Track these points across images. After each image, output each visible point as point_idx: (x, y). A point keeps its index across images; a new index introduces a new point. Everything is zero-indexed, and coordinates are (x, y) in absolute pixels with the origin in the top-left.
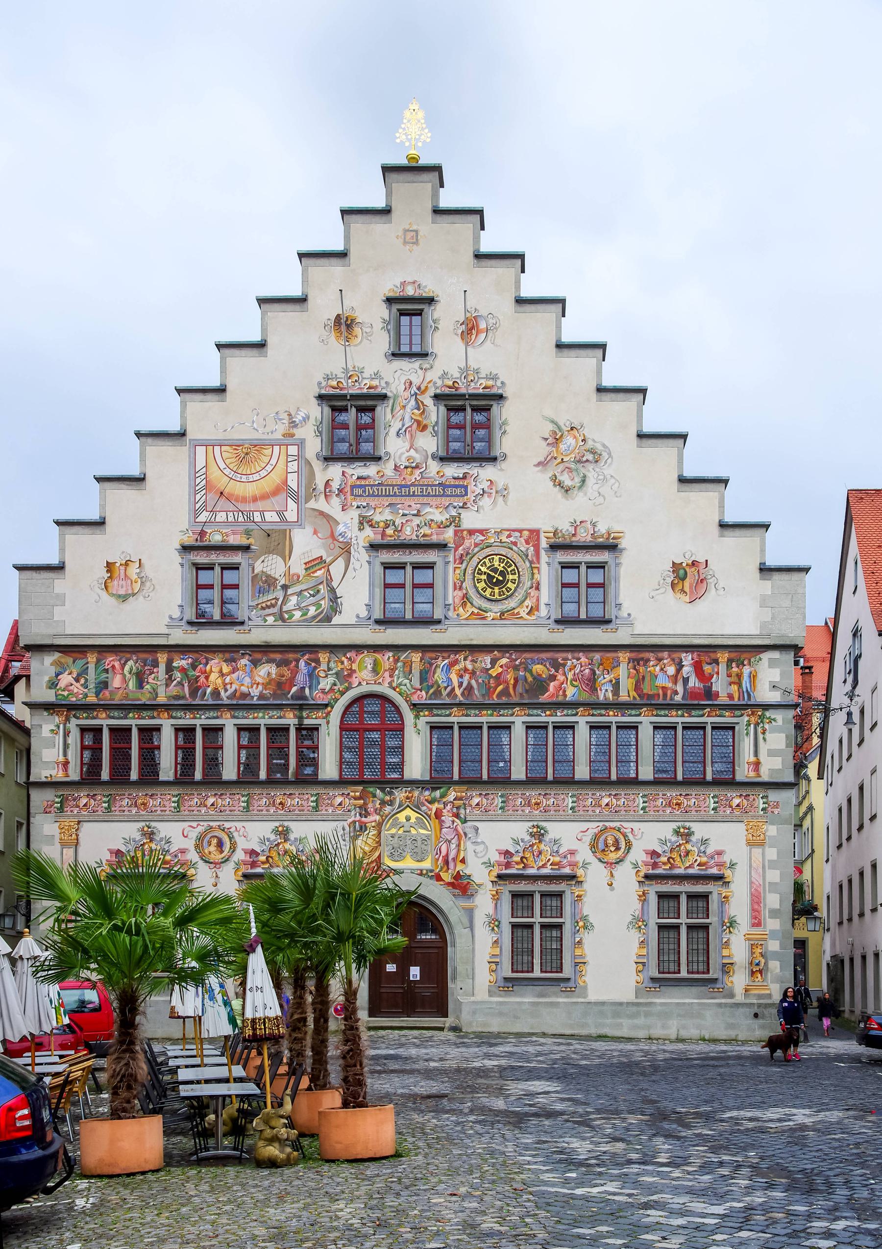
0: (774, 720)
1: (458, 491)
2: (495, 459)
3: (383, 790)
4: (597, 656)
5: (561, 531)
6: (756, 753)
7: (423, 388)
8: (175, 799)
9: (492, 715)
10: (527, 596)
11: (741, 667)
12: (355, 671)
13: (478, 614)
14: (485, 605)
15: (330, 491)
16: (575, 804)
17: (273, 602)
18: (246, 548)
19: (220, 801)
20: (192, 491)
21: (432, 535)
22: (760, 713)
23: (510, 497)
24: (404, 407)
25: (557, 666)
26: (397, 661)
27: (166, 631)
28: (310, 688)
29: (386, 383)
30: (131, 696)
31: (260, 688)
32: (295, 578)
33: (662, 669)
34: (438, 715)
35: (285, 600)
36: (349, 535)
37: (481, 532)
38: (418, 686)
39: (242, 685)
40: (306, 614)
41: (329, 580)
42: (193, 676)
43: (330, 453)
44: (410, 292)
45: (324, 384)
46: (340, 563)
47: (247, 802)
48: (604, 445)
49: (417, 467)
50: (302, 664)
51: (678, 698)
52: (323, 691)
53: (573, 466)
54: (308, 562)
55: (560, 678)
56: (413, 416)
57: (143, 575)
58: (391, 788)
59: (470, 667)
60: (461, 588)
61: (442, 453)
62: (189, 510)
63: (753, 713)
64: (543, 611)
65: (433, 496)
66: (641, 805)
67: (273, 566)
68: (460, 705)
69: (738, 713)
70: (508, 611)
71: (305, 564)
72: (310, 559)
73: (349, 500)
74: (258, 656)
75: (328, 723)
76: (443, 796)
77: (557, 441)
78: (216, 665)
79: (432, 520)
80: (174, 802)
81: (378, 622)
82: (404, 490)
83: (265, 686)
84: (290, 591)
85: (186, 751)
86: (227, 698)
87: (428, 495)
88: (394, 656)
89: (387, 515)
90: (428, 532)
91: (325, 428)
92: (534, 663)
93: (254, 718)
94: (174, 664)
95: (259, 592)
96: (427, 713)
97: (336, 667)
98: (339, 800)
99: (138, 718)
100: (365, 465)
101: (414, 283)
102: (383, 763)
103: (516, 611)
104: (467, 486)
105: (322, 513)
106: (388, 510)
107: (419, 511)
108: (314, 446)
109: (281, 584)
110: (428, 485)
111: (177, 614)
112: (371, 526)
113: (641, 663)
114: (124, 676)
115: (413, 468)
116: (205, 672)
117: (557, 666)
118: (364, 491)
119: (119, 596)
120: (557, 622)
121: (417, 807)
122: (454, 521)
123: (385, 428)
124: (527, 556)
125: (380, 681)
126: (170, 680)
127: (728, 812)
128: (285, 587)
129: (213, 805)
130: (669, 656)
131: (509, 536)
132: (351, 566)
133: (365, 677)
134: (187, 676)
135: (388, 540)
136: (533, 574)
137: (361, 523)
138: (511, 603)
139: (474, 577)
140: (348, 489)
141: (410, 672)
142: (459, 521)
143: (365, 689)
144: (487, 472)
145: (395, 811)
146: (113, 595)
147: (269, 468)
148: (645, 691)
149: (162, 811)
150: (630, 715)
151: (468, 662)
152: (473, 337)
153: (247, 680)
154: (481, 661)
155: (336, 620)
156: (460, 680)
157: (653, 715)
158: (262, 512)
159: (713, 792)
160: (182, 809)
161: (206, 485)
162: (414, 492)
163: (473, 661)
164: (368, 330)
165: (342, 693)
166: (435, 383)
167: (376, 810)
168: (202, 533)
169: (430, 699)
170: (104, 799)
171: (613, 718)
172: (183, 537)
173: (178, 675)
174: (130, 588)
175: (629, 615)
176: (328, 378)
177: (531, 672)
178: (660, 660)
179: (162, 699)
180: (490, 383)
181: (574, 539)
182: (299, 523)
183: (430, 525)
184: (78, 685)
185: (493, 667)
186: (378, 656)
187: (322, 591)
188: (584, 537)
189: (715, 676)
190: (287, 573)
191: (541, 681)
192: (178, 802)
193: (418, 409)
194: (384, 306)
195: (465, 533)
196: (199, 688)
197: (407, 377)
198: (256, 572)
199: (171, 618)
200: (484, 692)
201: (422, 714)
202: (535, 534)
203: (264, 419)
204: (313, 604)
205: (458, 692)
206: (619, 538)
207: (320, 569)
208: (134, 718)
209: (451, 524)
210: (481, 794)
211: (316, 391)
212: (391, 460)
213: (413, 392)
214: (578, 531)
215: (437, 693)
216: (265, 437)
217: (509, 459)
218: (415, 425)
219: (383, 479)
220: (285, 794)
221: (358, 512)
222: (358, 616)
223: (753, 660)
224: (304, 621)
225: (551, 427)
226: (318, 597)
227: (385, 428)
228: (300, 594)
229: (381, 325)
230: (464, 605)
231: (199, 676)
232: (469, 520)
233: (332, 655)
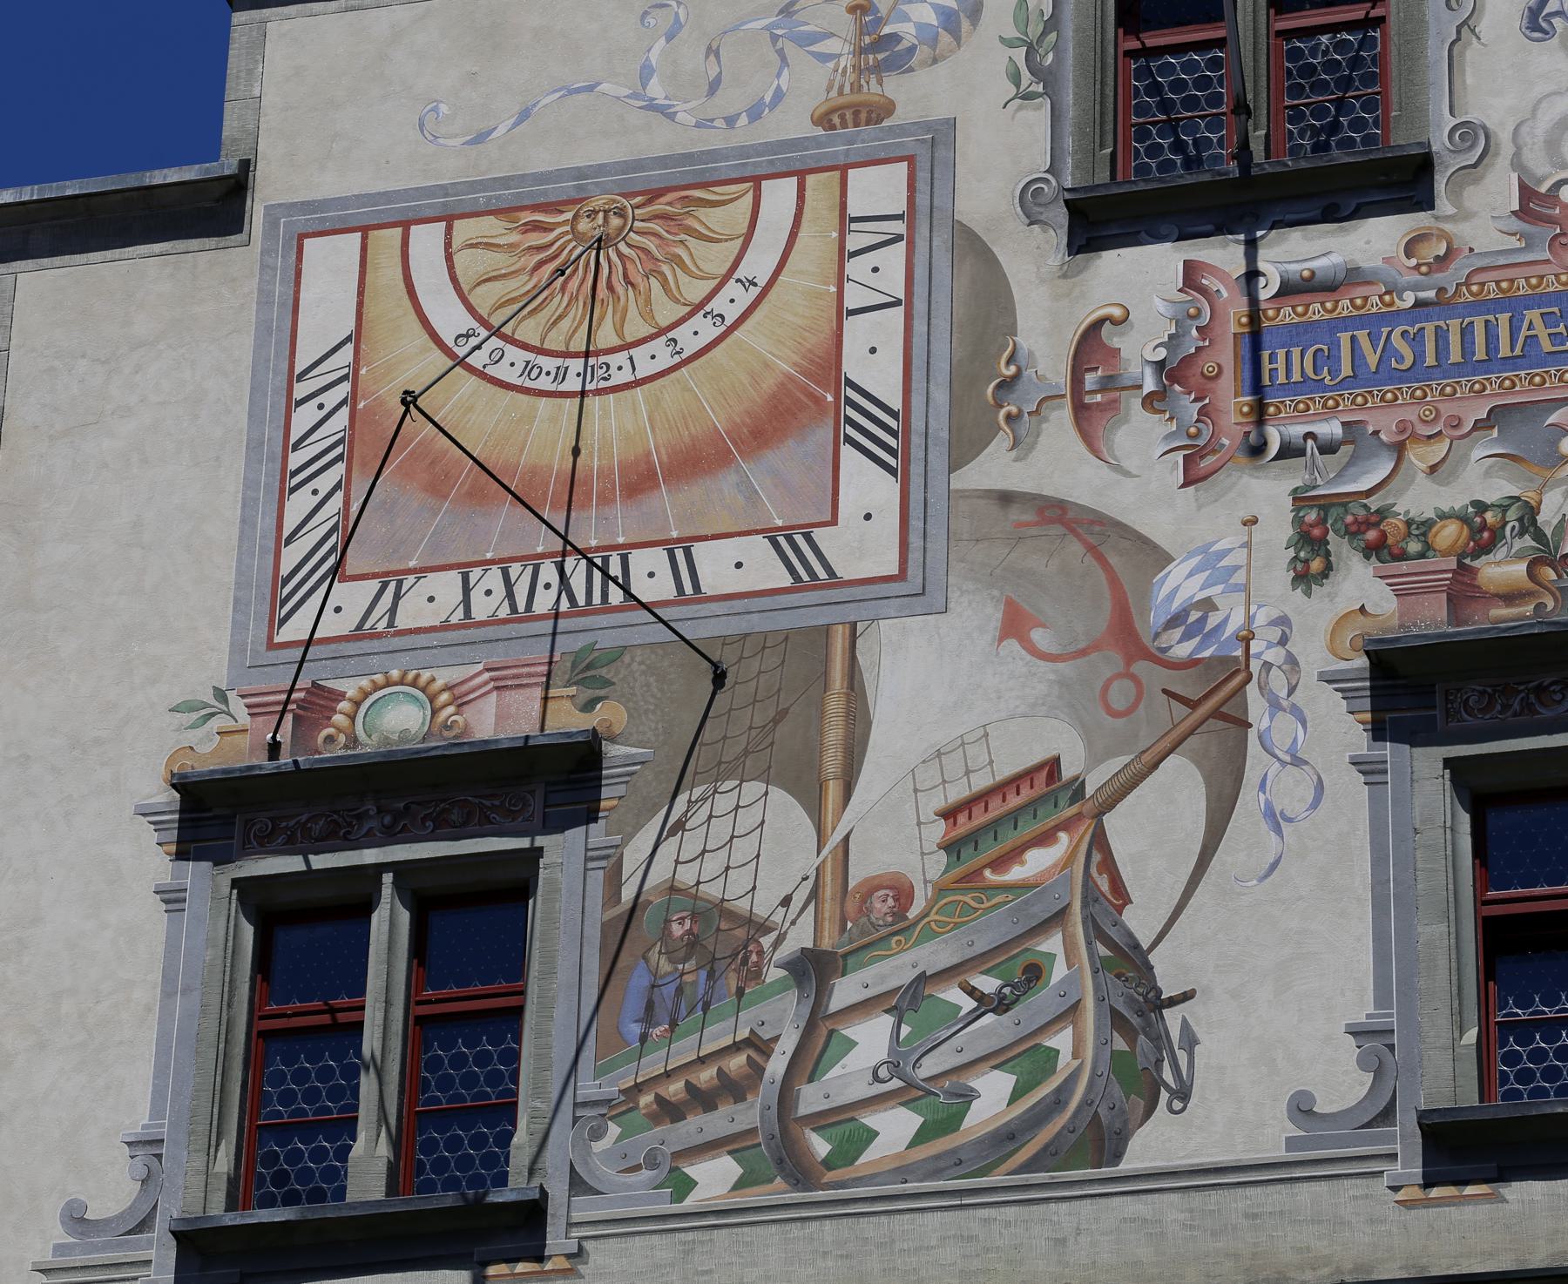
15: (1107, 384)
17: (737, 1063)
20: (267, 474)
32: (881, 906)
43: (1103, 176)
54: (967, 805)
62: (241, 584)
67: (743, 850)
71: (949, 814)
72: (981, 782)
84: (845, 992)
95: (649, 1015)
112: (1377, 550)
132: (1249, 801)
158: (680, 549)
161: (349, 439)
172: (192, 737)
187: (1059, 971)
199: (76, 1219)
203: (713, 52)
204: (996, 1059)
212: (1503, 161)
216: (715, 140)
219: (1450, 277)
221: (1292, 477)
222: (1302, 1109)
224: (935, 1168)
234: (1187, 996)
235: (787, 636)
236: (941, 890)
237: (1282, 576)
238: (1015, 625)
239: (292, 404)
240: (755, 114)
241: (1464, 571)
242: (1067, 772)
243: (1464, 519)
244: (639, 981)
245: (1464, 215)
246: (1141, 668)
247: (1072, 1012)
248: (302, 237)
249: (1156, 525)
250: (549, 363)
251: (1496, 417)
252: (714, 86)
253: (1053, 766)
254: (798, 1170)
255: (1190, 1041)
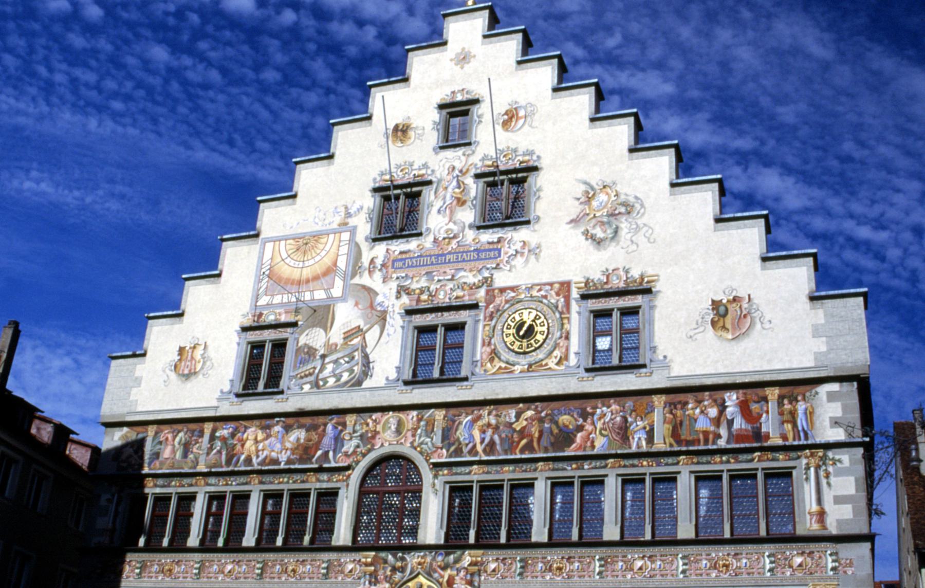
0: (840, 461)
1: (492, 254)
2: (528, 222)
3: (395, 556)
4: (629, 403)
5: (593, 281)
6: (819, 501)
7: (464, 170)
8: (197, 566)
9: (514, 471)
10: (556, 346)
11: (794, 403)
12: (378, 433)
13: (506, 368)
14: (512, 358)
16: (603, 569)
17: (311, 371)
18: (294, 325)
19: (236, 567)
20: (257, 280)
21: (464, 296)
22: (821, 454)
23: (542, 254)
24: (446, 188)
25: (585, 415)
26: (420, 420)
27: (215, 404)
28: (334, 451)
29: (433, 171)
30: (176, 466)
31: (289, 452)
32: (333, 347)
33: (702, 412)
34: (457, 474)
35: (323, 368)
36: (386, 304)
37: (512, 289)
38: (440, 445)
39: (273, 451)
40: (338, 380)
41: (364, 347)
42: (231, 444)
44: (459, 98)
45: (378, 179)
46: (376, 329)
47: (262, 569)
48: (636, 198)
49: (455, 237)
50: (329, 427)
51: (722, 443)
52: (346, 455)
53: (605, 219)
55: (589, 427)
56: (454, 195)
57: (206, 355)
58: (403, 554)
59: (493, 422)
60: (489, 344)
61: (478, 224)
63: (812, 455)
64: (573, 361)
65: (468, 261)
66: (681, 569)
67: (316, 338)
68: (480, 463)
69: (793, 454)
70: (536, 363)
71: (344, 333)
72: (349, 329)
73: (390, 273)
74: (291, 421)
75: (348, 485)
76: (457, 561)
77: (589, 200)
78: (252, 432)
79: (465, 283)
80: (196, 569)
81: (406, 383)
82: (440, 258)
83: (293, 451)
84: (327, 360)
85: (214, 517)
86: (259, 464)
87: (464, 261)
88: (417, 416)
89: (423, 283)
90: (460, 293)
91: (375, 216)
92: (561, 414)
93: (280, 483)
94: (218, 434)
95: (300, 364)
96: (446, 472)
97: (361, 429)
98: (350, 566)
99: (179, 486)
100: (407, 241)
101: (463, 90)
102: (400, 527)
103: (544, 363)
104: (499, 250)
105: (364, 287)
106: (424, 279)
107: (453, 276)
108: (364, 228)
109: (320, 354)
110: (463, 252)
111: (227, 388)
112: (408, 294)
113: (679, 406)
114: (173, 446)
115: (450, 238)
116: (242, 440)
117: (585, 415)
118: (404, 264)
119: (183, 375)
120: (588, 370)
121: (429, 575)
122: (486, 282)
123: (428, 208)
124: (557, 307)
125: (403, 441)
126: (211, 449)
127: (788, 574)
128: (323, 357)
129: (230, 572)
130: (711, 396)
131: (540, 290)
133: (388, 438)
134: (226, 443)
135: (422, 306)
136: (563, 324)
137: (398, 292)
138: (540, 355)
139: (503, 332)
140: (390, 263)
141: (433, 430)
142: (492, 281)
143: (387, 449)
144: (521, 235)
145: (405, 579)
146: (179, 375)
147: (323, 253)
148: (683, 437)
149: (184, 578)
150: (667, 464)
151: (491, 417)
152: (513, 124)
153: (278, 446)
154: (505, 416)
155: (366, 384)
156: (483, 436)
157: (693, 463)
159: (767, 549)
160: (202, 575)
162: (449, 260)
163: (497, 416)
164: (420, 132)
165: (364, 455)
166: (476, 165)
167: (386, 577)
168: (261, 315)
169: (450, 456)
170: (138, 565)
171: (647, 468)
173: (218, 444)
174: (193, 367)
175: (665, 357)
176: (382, 174)
177: (556, 423)
178: (699, 402)
179: (202, 468)
180: (527, 158)
181: (606, 286)
182: (343, 299)
183: (463, 287)
184: (136, 457)
185: (517, 420)
186: (402, 415)
187: (356, 358)
188: (618, 283)
189: (764, 415)
190: (327, 345)
191: (568, 433)
192: (199, 568)
193: (459, 187)
194: (436, 111)
195: (496, 291)
196: (232, 456)
197: (450, 164)
198: (300, 344)
199: (222, 392)
200: (506, 447)
201: (441, 473)
202: (565, 287)
203: (325, 214)
204: (347, 370)
205: (479, 448)
206: (653, 281)
207: (357, 337)
208: (175, 486)
209: (483, 284)
210: (497, 559)
211: (372, 185)
213: (455, 175)
214: (610, 279)
215: (458, 452)
217: (542, 221)
218: (455, 202)
219: (423, 251)
220: (298, 561)
222: (387, 379)
223: (808, 394)
224: (337, 387)
225: (583, 188)
226: (353, 363)
227: (428, 208)
228: (336, 362)
229: (432, 126)
230: (492, 360)
231: (236, 445)
232: (501, 279)
233: (359, 418)
234: (373, 362)
235: (325, 306)
236: (342, 345)
237: (394, 297)
238: (357, 304)
239: (262, 269)
240: (330, 224)
241: (419, 297)
242: (361, 327)
243: (419, 289)
244: (300, 358)
245: (425, 242)
246: (373, 312)
247: (357, 364)
248: (265, 243)
249: (377, 289)
250: (297, 263)
251: (427, 273)
252: (324, 220)
253: (359, 327)
254: (318, 386)
255: (373, 368)
